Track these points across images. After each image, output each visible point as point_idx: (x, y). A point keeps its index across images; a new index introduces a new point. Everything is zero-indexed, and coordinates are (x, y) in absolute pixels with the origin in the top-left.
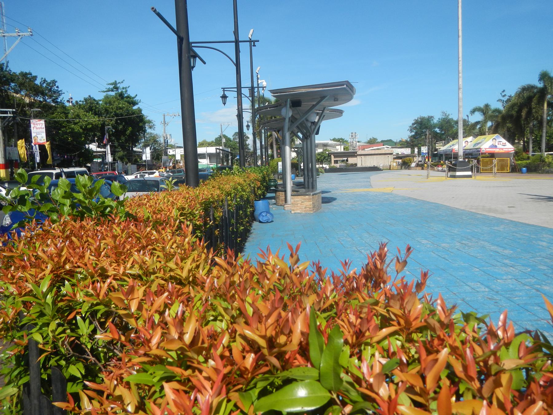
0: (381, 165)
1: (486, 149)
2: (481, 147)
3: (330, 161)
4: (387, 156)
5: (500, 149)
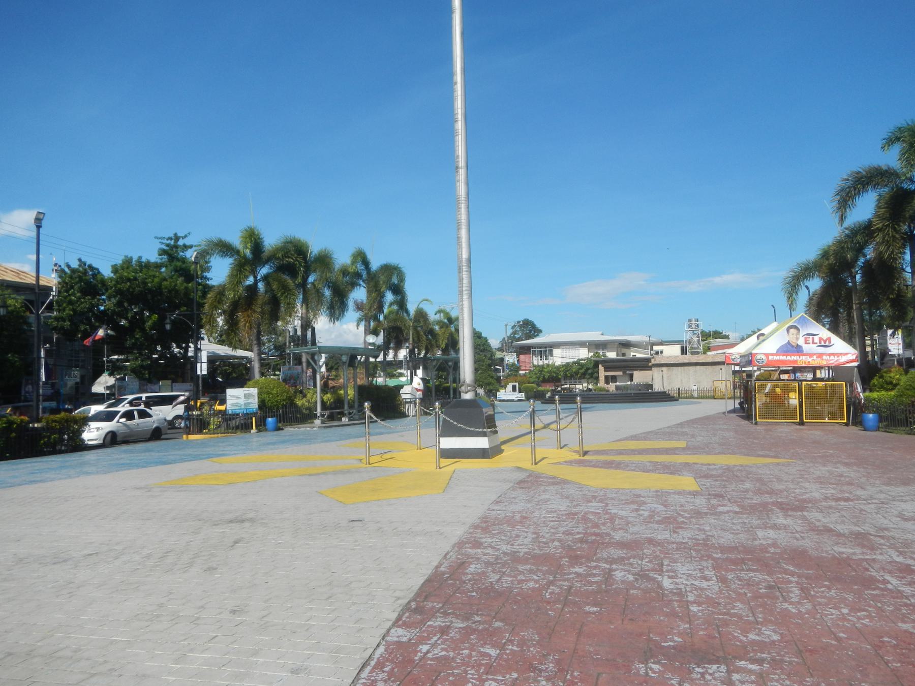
1: (767, 355)
2: (754, 352)
3: (597, 378)
5: (811, 355)
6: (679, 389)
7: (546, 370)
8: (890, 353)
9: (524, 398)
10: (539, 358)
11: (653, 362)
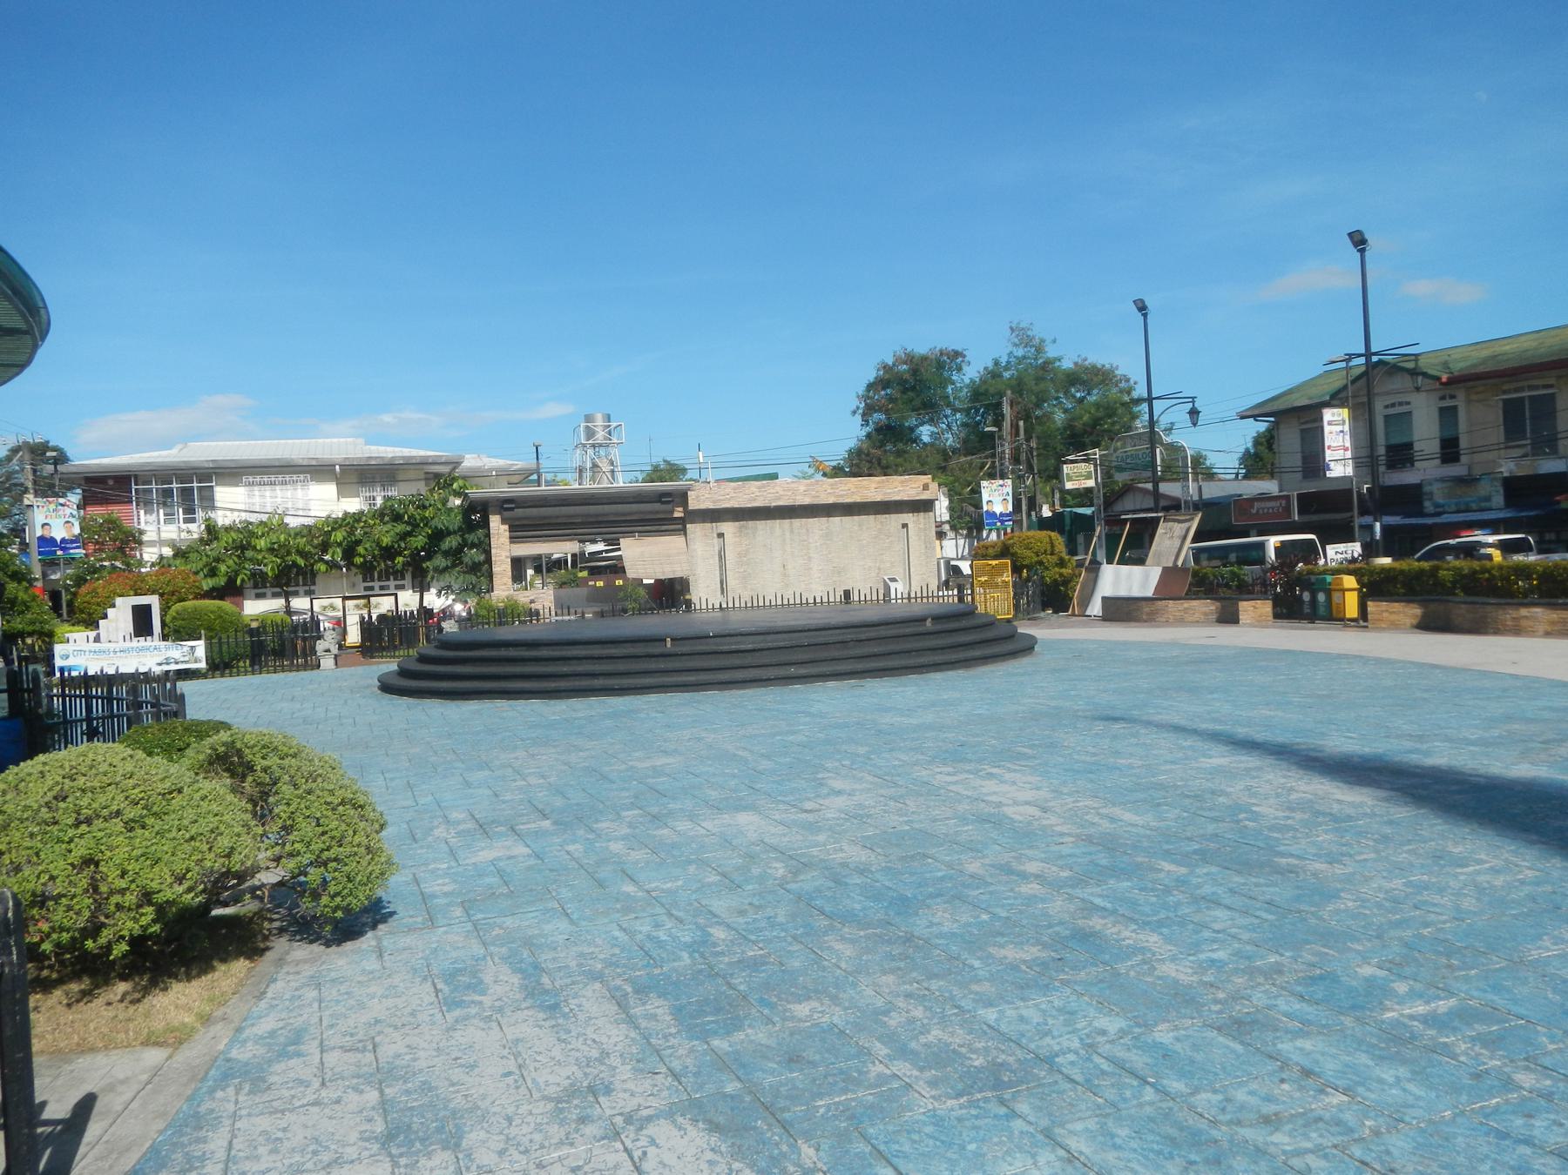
0: (899, 588)
3: (483, 569)
4: (895, 520)
6: (847, 594)
7: (262, 543)
8: (1328, 474)
9: (203, 665)
11: (694, 503)
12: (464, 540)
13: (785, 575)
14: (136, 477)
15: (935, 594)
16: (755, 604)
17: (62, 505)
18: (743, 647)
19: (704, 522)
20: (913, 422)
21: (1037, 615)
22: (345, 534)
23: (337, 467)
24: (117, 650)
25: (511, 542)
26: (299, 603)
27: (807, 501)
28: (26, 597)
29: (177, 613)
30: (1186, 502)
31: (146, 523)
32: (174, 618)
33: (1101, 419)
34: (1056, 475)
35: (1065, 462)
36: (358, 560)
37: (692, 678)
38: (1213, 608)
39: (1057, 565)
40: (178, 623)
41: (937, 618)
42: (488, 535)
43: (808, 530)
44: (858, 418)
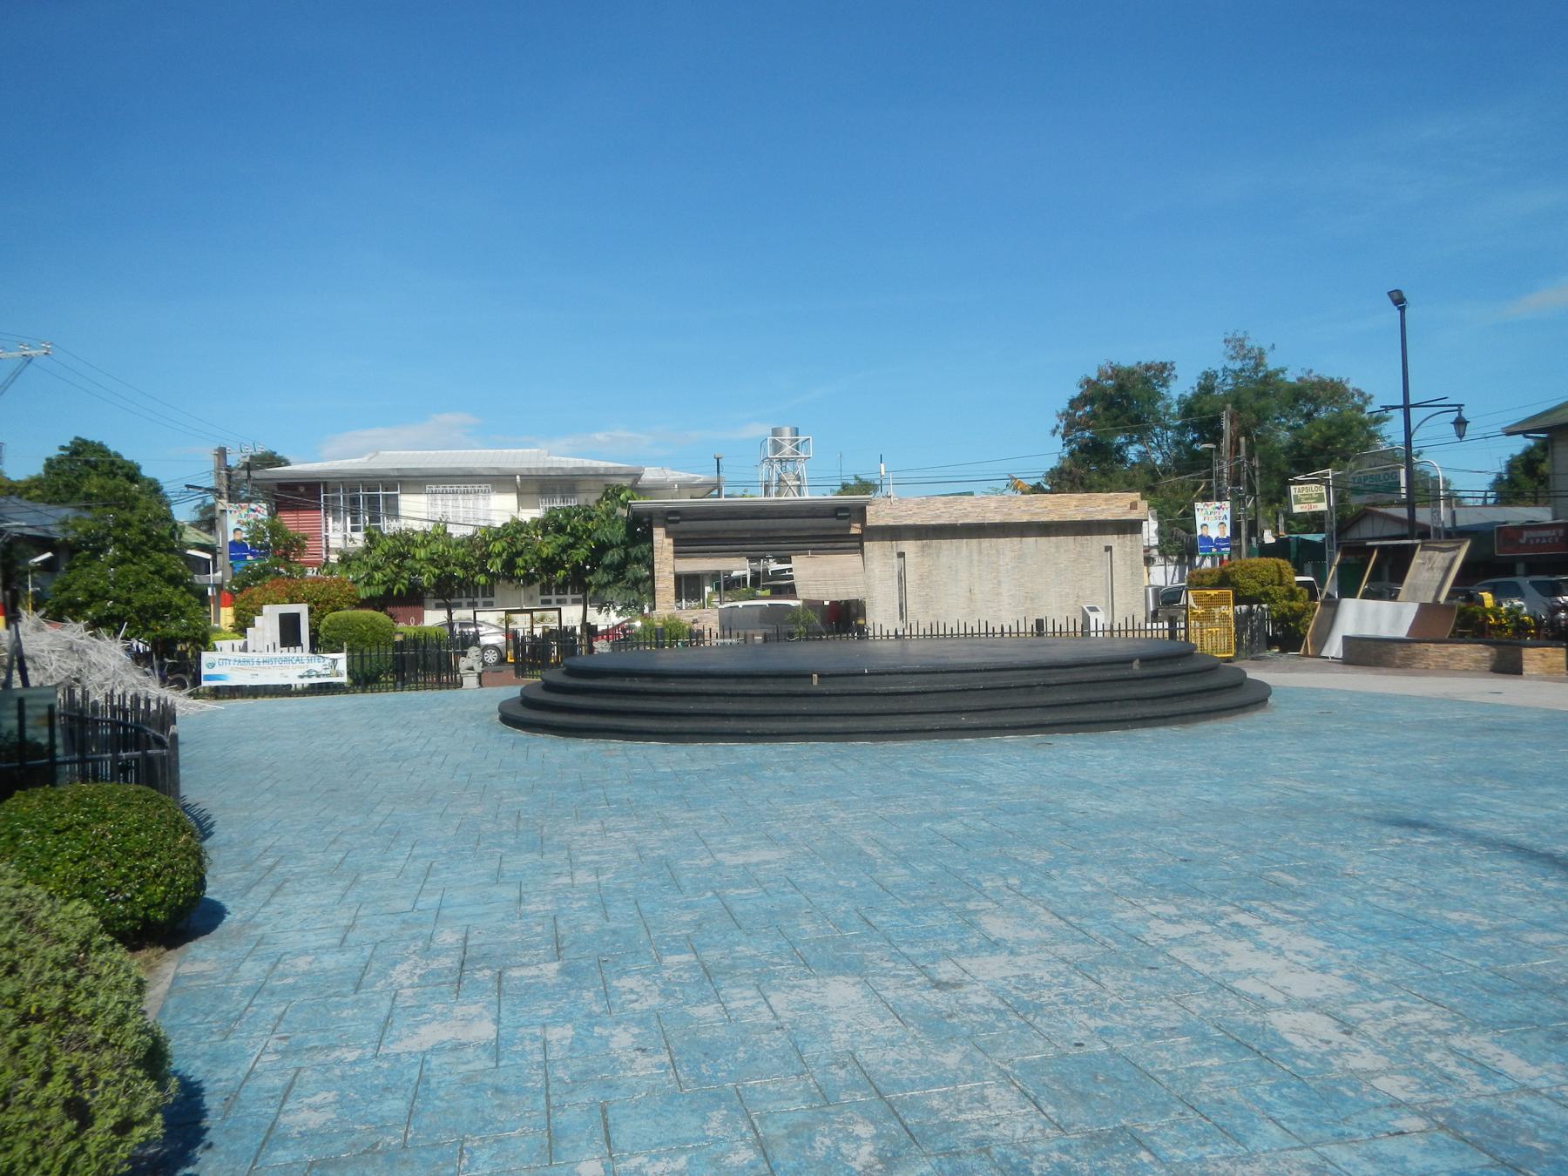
0: (1099, 619)
3: (645, 587)
4: (1098, 542)
7: (421, 553)
9: (344, 679)
10: (349, 525)
11: (871, 521)
12: (627, 554)
13: (971, 600)
14: (325, 484)
15: (1143, 627)
16: (935, 632)
17: (254, 511)
18: (904, 688)
19: (883, 539)
20: (1120, 439)
21: (1263, 654)
22: (505, 544)
23: (518, 477)
24: (261, 660)
25: (675, 558)
26: (462, 614)
27: (998, 519)
28: (181, 603)
29: (329, 623)
30: (1436, 530)
31: (334, 530)
32: (326, 628)
33: (1334, 438)
34: (1282, 496)
35: (1294, 483)
36: (520, 572)
37: (838, 725)
38: (1487, 654)
39: (1285, 597)
40: (332, 633)
41: (1146, 660)
42: (652, 550)
43: (998, 551)
44: (1058, 436)
